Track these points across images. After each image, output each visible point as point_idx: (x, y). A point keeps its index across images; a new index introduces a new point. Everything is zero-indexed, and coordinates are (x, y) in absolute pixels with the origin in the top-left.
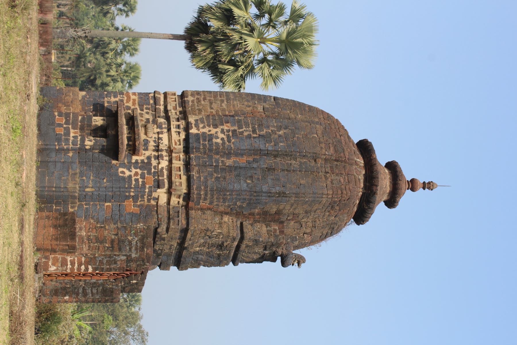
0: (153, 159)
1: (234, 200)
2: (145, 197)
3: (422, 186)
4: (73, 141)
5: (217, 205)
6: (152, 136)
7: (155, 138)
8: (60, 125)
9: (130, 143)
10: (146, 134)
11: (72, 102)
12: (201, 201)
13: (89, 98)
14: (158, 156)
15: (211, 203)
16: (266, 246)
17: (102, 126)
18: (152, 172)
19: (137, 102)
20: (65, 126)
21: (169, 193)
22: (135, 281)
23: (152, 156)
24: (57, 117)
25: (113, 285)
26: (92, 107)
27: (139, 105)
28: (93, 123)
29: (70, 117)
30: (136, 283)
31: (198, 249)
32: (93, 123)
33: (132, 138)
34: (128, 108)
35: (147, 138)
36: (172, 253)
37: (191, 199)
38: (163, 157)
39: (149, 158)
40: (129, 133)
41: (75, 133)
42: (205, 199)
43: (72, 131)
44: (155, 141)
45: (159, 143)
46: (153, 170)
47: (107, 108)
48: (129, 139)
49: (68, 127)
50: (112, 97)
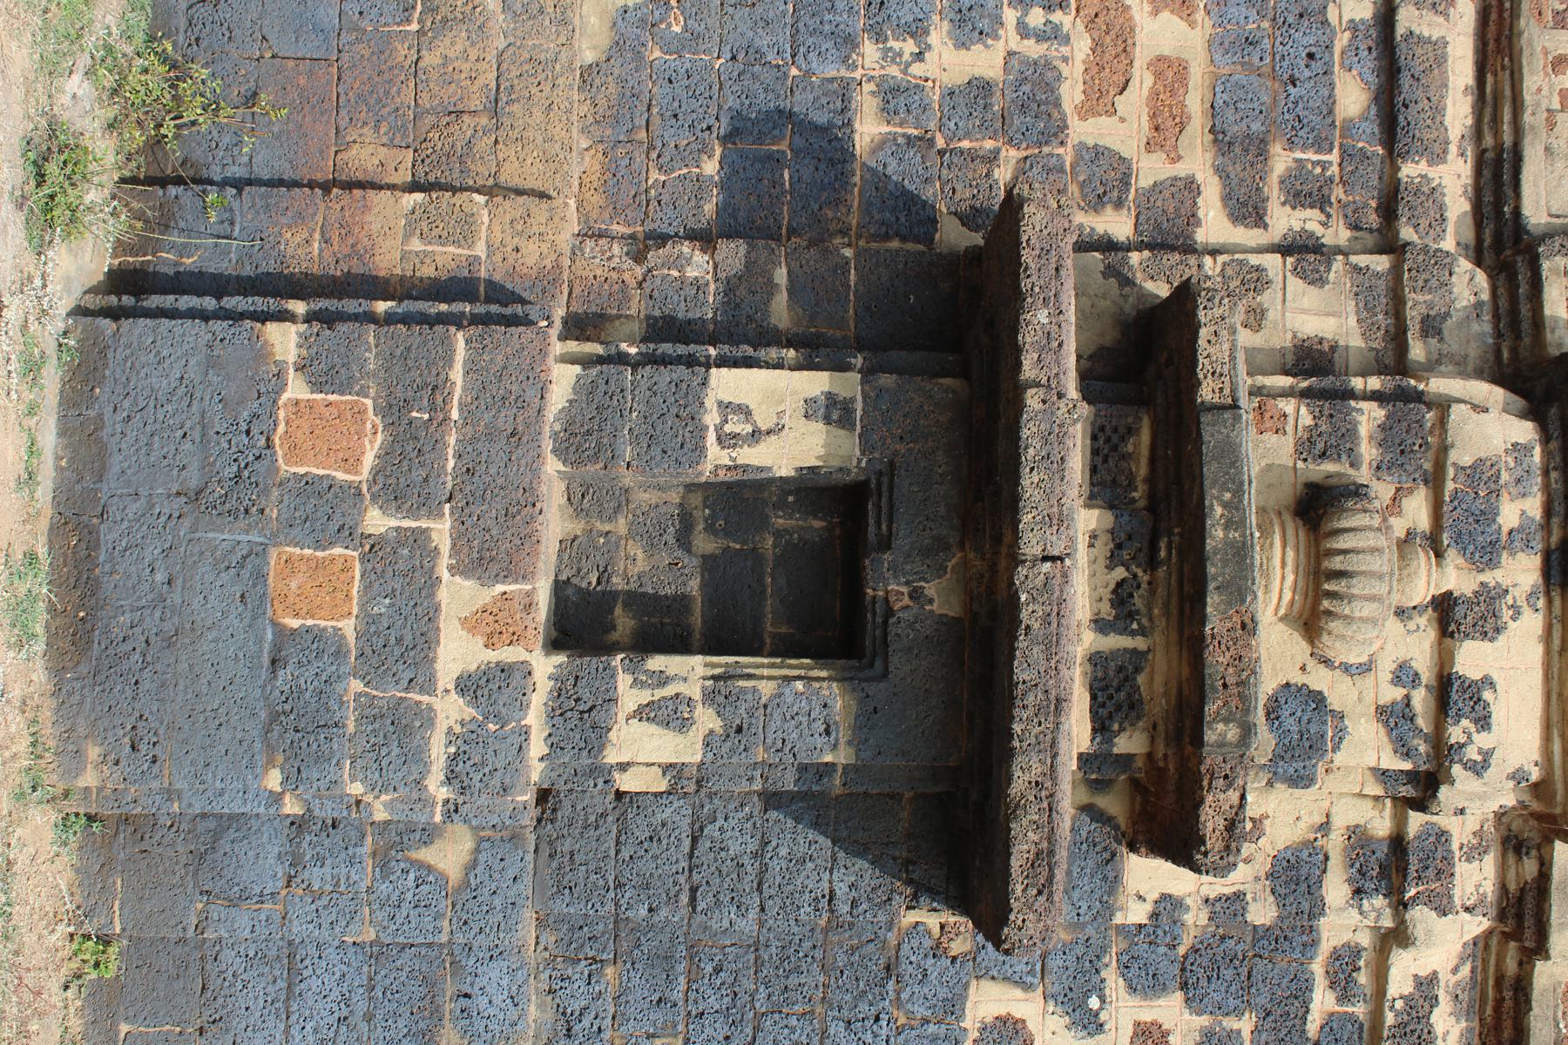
0: (1336, 889)
4: (466, 743)
6: (1384, 642)
7: (1404, 675)
8: (323, 510)
9: (1129, 743)
10: (1311, 621)
11: (494, 108)
13: (693, 38)
14: (1398, 843)
17: (810, 489)
18: (1312, 1028)
19: (1195, 102)
20: (377, 521)
23: (1335, 844)
24: (296, 389)
26: (711, 167)
27: (1220, 139)
28: (716, 456)
29: (436, 389)
32: (716, 456)
33: (1154, 685)
34: (1107, 179)
35: (1319, 679)
38: (1445, 873)
39: (1296, 876)
40: (1121, 609)
41: (493, 625)
43: (458, 595)
44: (1394, 718)
45: (1443, 754)
46: (1322, 1002)
47: (877, 179)
48: (1114, 694)
49: (419, 538)
50: (939, 35)
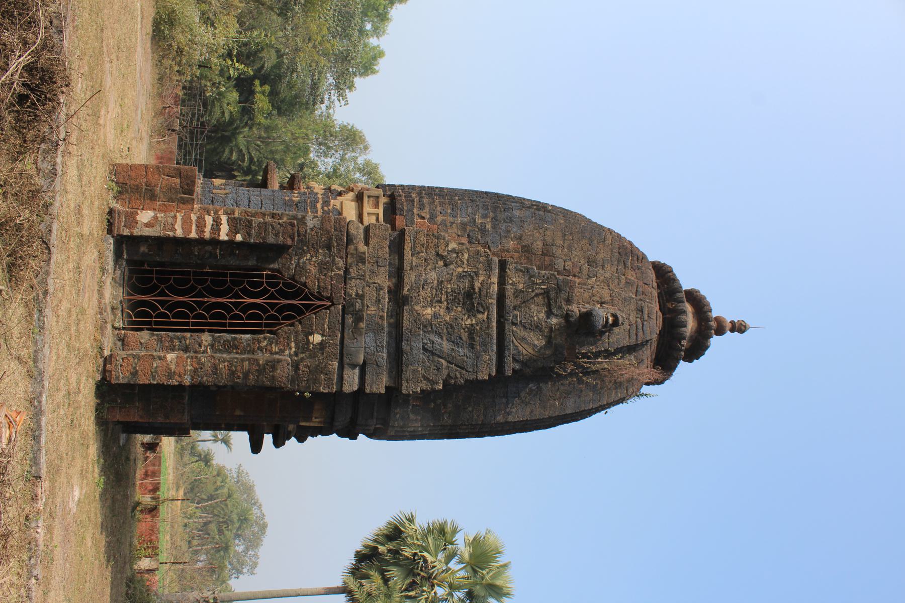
1: (470, 210)
2: (319, 206)
3: (729, 326)
5: (443, 223)
12: (415, 211)
15: (432, 218)
16: (546, 293)
21: (359, 198)
22: (317, 338)
25: (271, 353)
30: (322, 345)
31: (429, 311)
36: (382, 317)
37: (398, 206)
42: (422, 207)
